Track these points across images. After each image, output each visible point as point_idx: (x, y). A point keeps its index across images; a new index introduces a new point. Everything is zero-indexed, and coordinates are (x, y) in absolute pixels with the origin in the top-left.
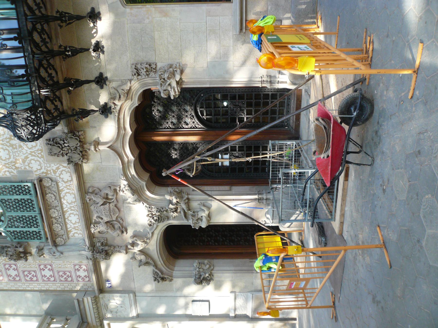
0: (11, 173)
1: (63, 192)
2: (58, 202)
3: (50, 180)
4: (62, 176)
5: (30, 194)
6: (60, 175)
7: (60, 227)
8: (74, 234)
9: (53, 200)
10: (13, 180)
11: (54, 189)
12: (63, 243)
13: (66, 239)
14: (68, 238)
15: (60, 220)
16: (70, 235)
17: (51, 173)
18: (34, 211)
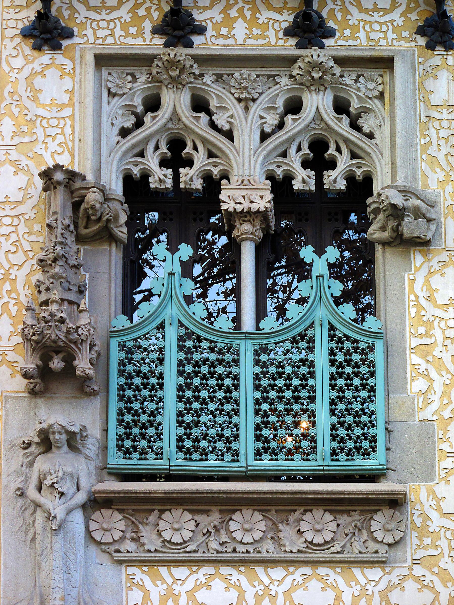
0: (421, 399)
1: (341, 581)
2: (299, 551)
3: (397, 539)
4: (410, 585)
5: (334, 453)
6: (418, 579)
7: (177, 539)
8: (141, 587)
9: (309, 536)
10: (394, 398)
11: (357, 546)
12: (97, 536)
13: (118, 551)
14: (120, 562)
15: (214, 545)
16: (131, 570)
17: (426, 547)
18: (258, 453)
